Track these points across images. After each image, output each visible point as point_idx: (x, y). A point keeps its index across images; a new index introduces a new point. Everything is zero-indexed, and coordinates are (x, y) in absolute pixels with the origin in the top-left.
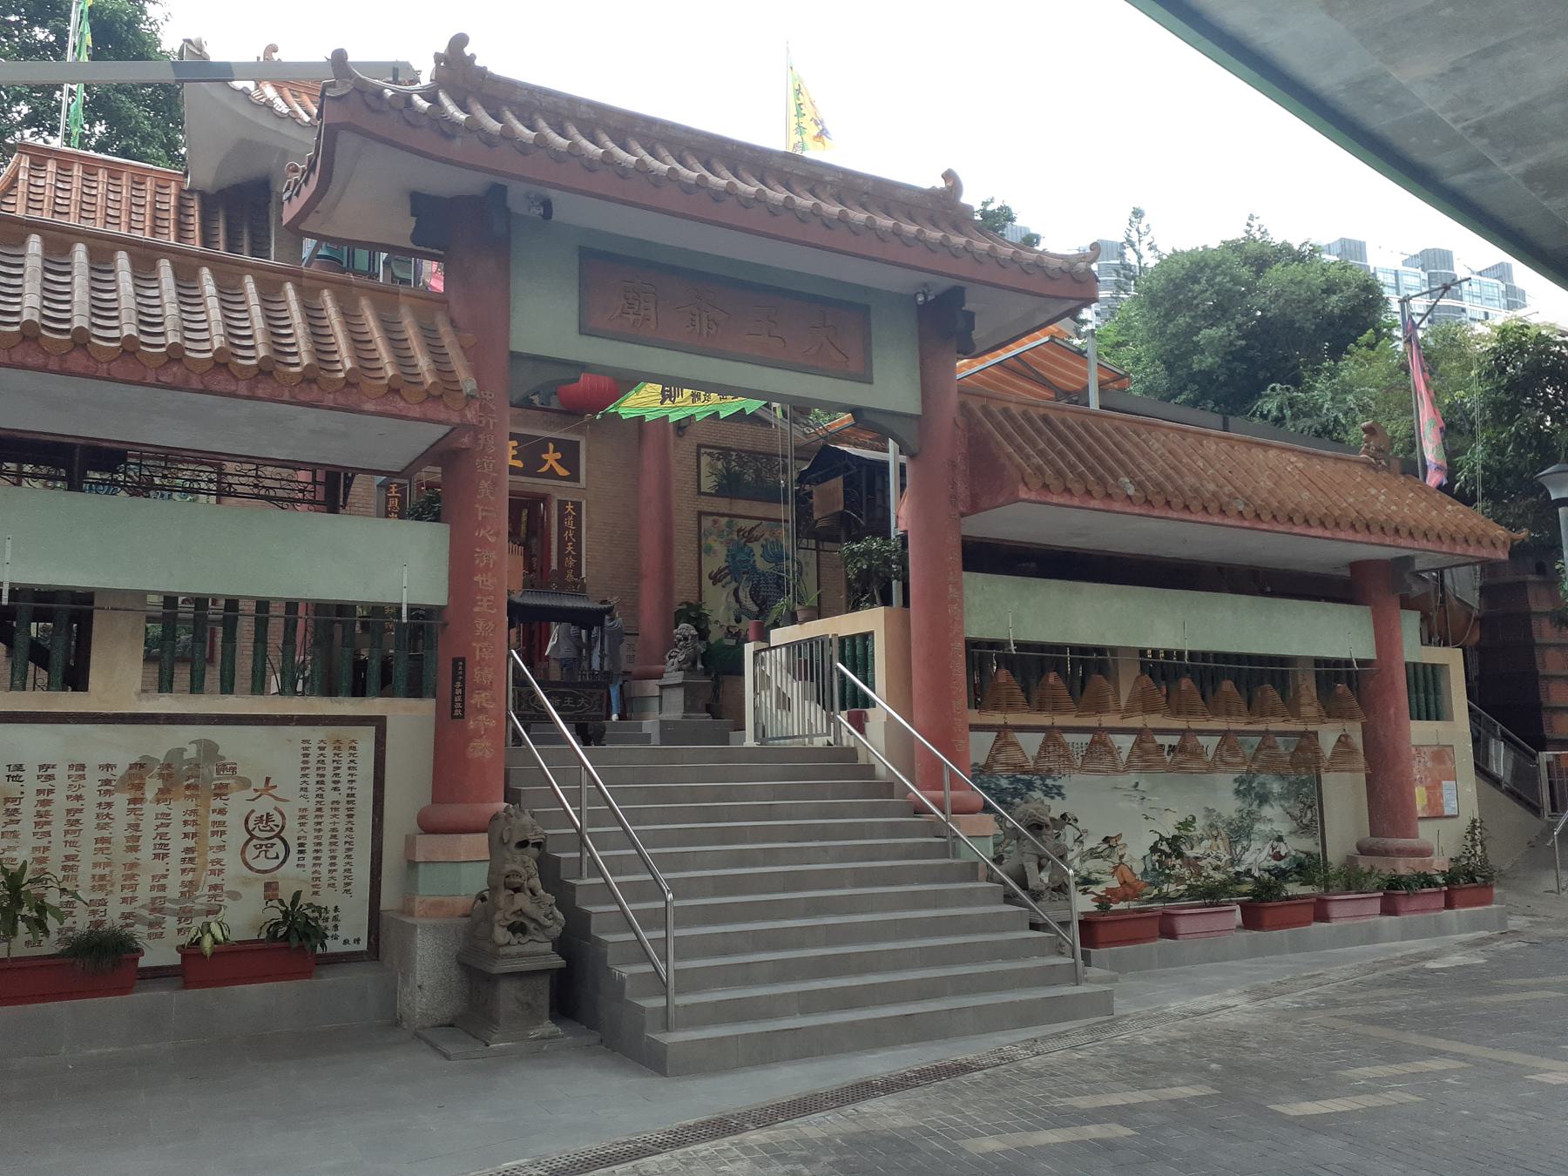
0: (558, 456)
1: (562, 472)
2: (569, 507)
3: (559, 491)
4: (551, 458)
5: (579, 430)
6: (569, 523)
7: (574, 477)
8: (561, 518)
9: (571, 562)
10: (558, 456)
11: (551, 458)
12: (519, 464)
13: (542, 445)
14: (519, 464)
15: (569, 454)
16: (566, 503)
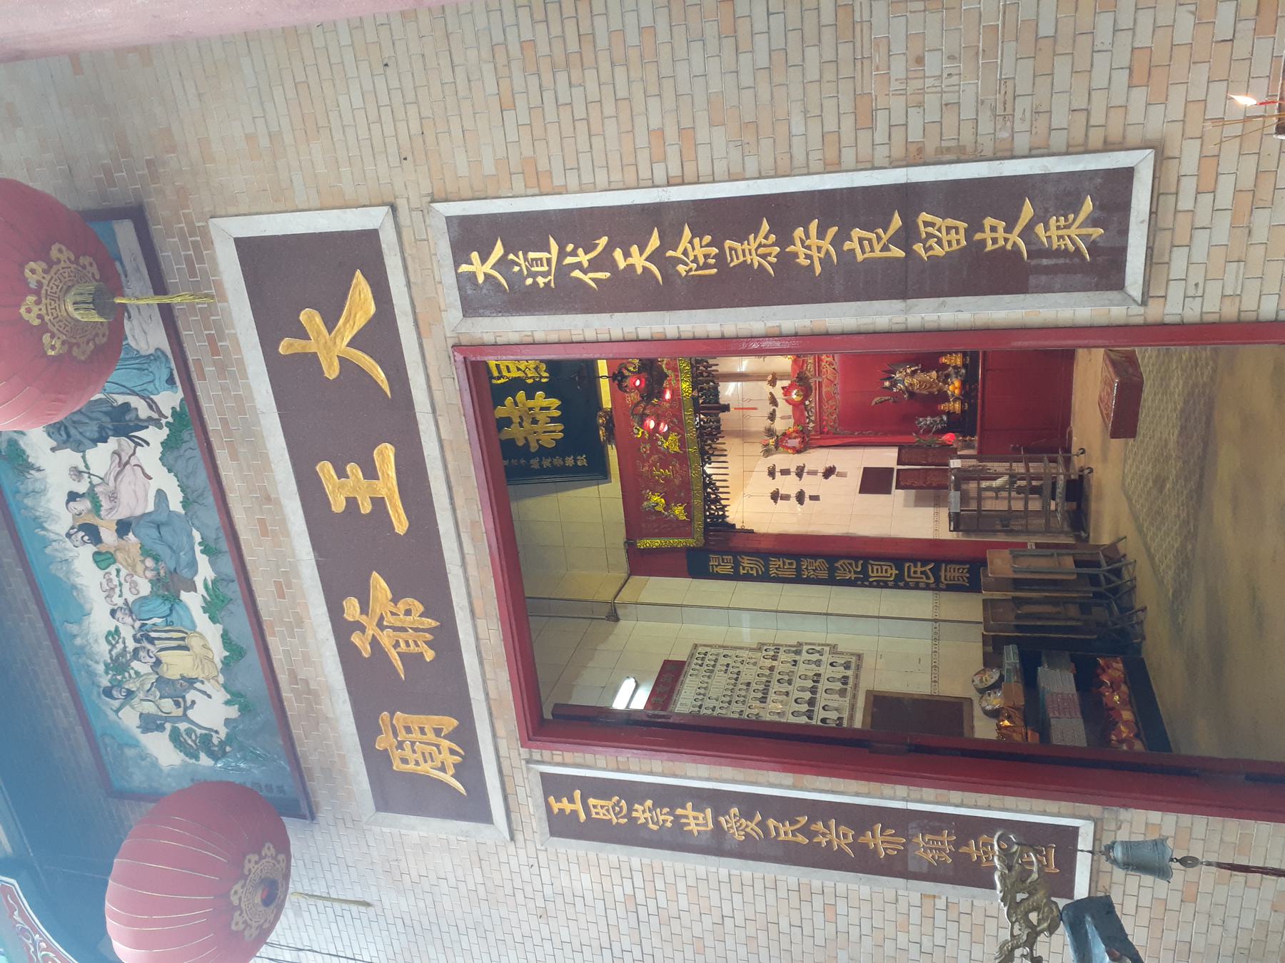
0: (310, 318)
1: (361, 303)
2: (479, 268)
3: (435, 319)
4: (331, 344)
5: (201, 244)
6: (539, 265)
7: (360, 252)
8: (522, 299)
9: (693, 252)
10: (310, 318)
11: (331, 344)
12: (385, 456)
13: (293, 378)
14: (385, 456)
15: (294, 276)
16: (466, 281)
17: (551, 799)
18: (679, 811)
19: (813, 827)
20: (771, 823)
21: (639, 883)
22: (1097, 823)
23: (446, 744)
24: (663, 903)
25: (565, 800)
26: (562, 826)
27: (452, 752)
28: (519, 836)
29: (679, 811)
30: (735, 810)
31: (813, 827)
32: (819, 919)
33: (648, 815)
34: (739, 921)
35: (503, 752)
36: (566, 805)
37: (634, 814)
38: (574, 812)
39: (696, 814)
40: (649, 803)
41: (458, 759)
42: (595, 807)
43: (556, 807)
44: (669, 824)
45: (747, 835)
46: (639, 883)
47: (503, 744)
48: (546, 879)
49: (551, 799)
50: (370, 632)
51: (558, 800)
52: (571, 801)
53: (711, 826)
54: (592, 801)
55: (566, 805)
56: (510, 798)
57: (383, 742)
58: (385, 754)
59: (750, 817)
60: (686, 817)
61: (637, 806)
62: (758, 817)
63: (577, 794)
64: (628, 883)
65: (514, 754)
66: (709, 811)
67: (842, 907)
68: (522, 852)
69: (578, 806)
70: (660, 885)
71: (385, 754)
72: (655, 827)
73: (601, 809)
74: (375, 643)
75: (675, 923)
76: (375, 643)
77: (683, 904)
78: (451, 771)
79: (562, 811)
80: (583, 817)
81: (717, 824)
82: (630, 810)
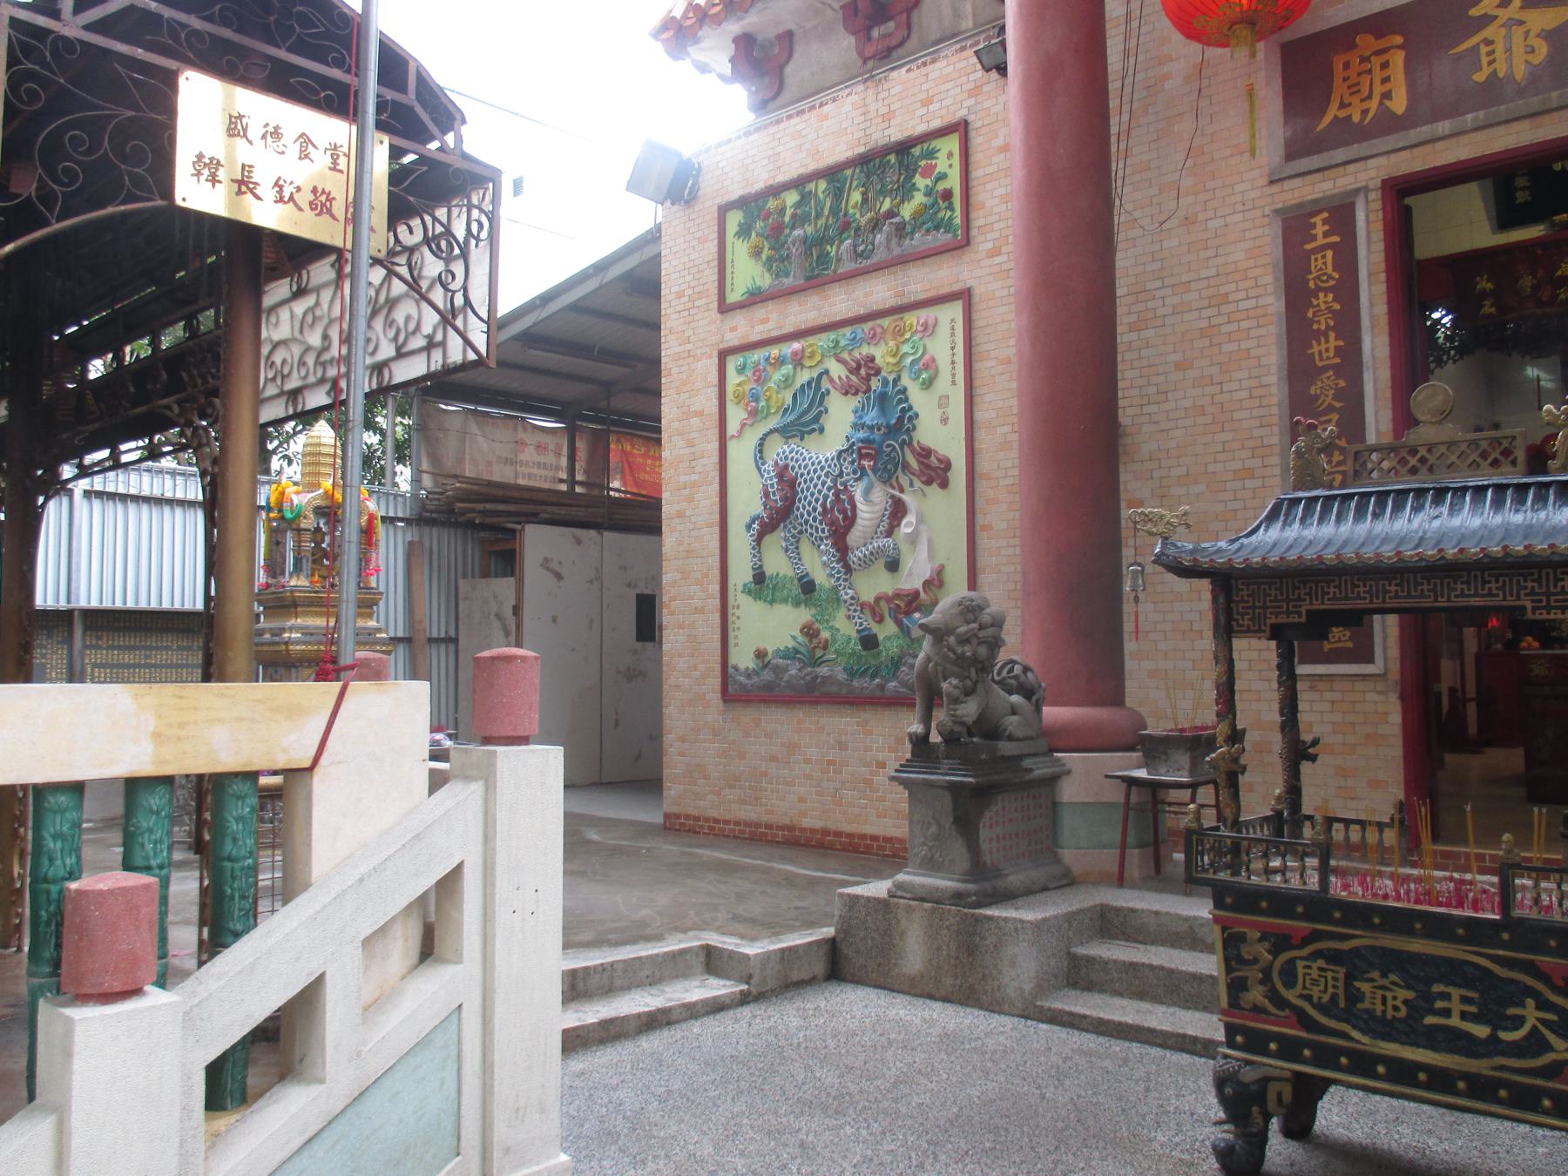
17: (1325, 215)
18: (1332, 335)
19: (1336, 453)
20: (1335, 417)
21: (1242, 305)
22: (1382, 677)
23: (1373, 105)
24: (1224, 329)
25: (1326, 227)
26: (1295, 225)
27: (1365, 112)
28: (1276, 188)
29: (1332, 335)
30: (1342, 383)
31: (1336, 453)
32: (1238, 465)
33: (1323, 307)
34: (1217, 399)
35: (1371, 163)
36: (1320, 230)
37: (1321, 295)
38: (1314, 238)
39: (1332, 350)
40: (1337, 307)
41: (1356, 118)
42: (1324, 257)
43: (1317, 220)
44: (1315, 327)
45: (1316, 397)
46: (1242, 305)
47: (1382, 161)
48: (1229, 219)
49: (1325, 215)
50: (1499, 12)
51: (1325, 222)
52: (1326, 235)
53: (1320, 364)
54: (1329, 253)
55: (1320, 230)
56: (1319, 176)
57: (1366, 42)
58: (1352, 46)
59: (1335, 398)
60: (1327, 341)
61: (1331, 296)
62: (1338, 405)
63: (1336, 239)
64: (1242, 295)
65: (1373, 173)
66: (1337, 360)
67: (1249, 484)
68: (1257, 193)
69: (1320, 241)
70: (1244, 325)
71: (1352, 46)
72: (1310, 314)
73: (1324, 264)
74: (1487, 20)
75: (1206, 342)
76: (1487, 20)
77: (1226, 348)
78: (1342, 114)
79: (1314, 226)
80: (1308, 247)
81: (1325, 369)
82: (1326, 291)
